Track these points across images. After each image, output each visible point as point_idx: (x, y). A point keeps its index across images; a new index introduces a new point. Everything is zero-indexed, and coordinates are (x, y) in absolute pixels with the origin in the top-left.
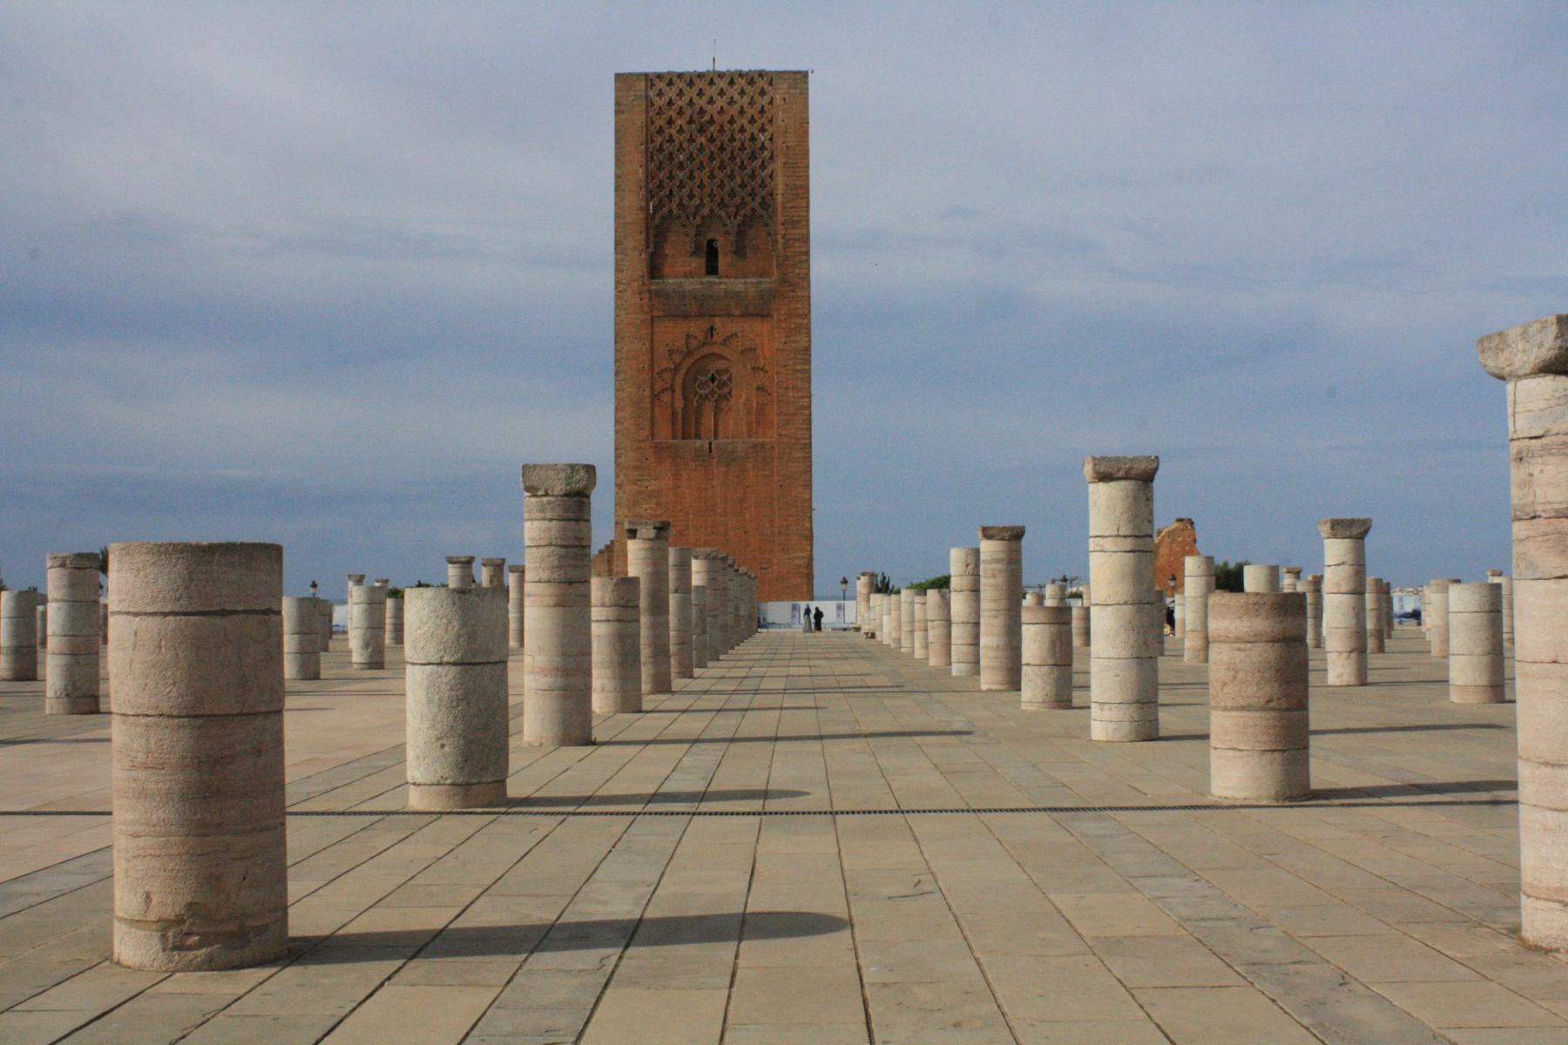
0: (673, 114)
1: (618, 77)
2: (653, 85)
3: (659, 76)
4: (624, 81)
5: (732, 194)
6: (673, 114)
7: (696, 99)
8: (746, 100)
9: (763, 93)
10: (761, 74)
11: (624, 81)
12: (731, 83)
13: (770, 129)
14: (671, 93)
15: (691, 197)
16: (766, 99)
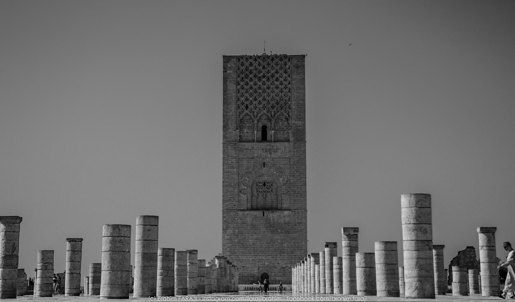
0: (248, 72)
1: (224, 57)
2: (239, 60)
3: (242, 57)
4: (227, 59)
5: (273, 107)
6: (248, 72)
7: (257, 67)
8: (279, 66)
9: (286, 64)
10: (285, 56)
11: (227, 59)
12: (273, 60)
13: (289, 79)
14: (247, 64)
15: (255, 108)
16: (287, 66)
